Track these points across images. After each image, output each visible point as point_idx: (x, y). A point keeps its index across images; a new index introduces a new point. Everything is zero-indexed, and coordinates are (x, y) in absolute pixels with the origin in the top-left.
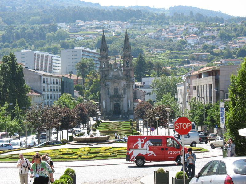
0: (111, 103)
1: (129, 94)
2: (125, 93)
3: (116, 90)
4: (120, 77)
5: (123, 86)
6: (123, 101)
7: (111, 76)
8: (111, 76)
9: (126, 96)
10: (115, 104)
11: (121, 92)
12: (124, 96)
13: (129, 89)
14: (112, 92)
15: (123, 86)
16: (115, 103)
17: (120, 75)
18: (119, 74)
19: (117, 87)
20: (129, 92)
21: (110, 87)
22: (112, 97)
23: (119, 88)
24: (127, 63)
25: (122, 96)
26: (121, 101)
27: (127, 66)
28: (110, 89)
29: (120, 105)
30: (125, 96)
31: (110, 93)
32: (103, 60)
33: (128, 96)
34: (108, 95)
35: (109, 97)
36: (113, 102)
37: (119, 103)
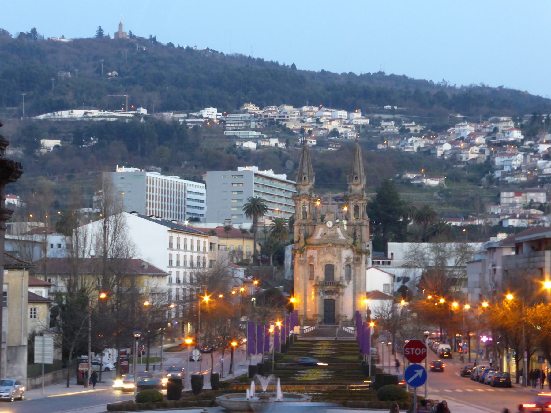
0: (318, 297)
2: (348, 277)
3: (329, 269)
4: (338, 241)
5: (344, 260)
6: (343, 294)
9: (351, 282)
10: (325, 300)
11: (340, 272)
12: (345, 283)
13: (358, 268)
14: (320, 273)
16: (327, 297)
18: (336, 233)
19: (331, 263)
20: (357, 277)
21: (316, 260)
22: (320, 286)
23: (335, 264)
25: (341, 283)
26: (339, 295)
28: (316, 266)
29: (336, 302)
30: (348, 283)
31: (316, 275)
32: (301, 202)
34: (310, 279)
35: (314, 284)
36: (322, 295)
37: (334, 297)
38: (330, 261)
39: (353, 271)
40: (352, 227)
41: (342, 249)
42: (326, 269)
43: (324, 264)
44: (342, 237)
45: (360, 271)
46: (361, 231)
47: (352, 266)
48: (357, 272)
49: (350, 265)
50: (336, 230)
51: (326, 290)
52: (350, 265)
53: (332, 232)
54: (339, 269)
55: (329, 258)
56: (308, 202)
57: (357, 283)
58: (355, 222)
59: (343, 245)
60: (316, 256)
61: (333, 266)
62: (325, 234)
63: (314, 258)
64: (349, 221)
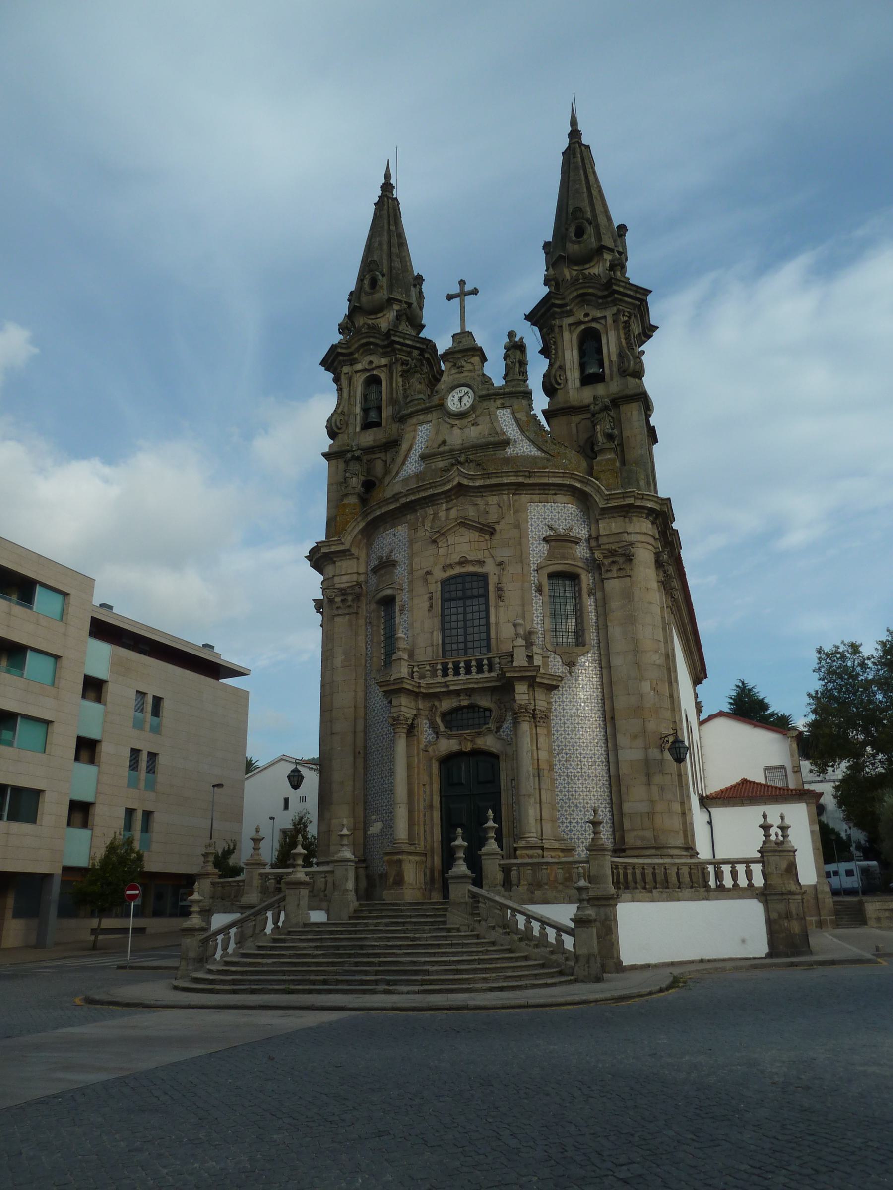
1: (619, 644)
5: (537, 552)
6: (540, 718)
7: (412, 466)
8: (412, 466)
11: (522, 614)
12: (556, 666)
15: (544, 548)
16: (448, 745)
17: (506, 443)
19: (471, 569)
20: (615, 631)
21: (401, 572)
23: (490, 568)
24: (590, 342)
27: (588, 380)
29: (504, 766)
32: (359, 367)
33: (605, 666)
37: (488, 742)
38: (463, 562)
39: (590, 604)
40: (576, 419)
42: (444, 600)
43: (439, 575)
44: (524, 448)
45: (628, 596)
46: (618, 423)
47: (586, 580)
48: (615, 604)
49: (573, 577)
50: (493, 420)
51: (446, 705)
52: (573, 577)
53: (474, 434)
54: (512, 590)
55: (463, 545)
56: (383, 361)
57: (617, 661)
58: (587, 395)
61: (484, 577)
62: (444, 442)
64: (560, 395)
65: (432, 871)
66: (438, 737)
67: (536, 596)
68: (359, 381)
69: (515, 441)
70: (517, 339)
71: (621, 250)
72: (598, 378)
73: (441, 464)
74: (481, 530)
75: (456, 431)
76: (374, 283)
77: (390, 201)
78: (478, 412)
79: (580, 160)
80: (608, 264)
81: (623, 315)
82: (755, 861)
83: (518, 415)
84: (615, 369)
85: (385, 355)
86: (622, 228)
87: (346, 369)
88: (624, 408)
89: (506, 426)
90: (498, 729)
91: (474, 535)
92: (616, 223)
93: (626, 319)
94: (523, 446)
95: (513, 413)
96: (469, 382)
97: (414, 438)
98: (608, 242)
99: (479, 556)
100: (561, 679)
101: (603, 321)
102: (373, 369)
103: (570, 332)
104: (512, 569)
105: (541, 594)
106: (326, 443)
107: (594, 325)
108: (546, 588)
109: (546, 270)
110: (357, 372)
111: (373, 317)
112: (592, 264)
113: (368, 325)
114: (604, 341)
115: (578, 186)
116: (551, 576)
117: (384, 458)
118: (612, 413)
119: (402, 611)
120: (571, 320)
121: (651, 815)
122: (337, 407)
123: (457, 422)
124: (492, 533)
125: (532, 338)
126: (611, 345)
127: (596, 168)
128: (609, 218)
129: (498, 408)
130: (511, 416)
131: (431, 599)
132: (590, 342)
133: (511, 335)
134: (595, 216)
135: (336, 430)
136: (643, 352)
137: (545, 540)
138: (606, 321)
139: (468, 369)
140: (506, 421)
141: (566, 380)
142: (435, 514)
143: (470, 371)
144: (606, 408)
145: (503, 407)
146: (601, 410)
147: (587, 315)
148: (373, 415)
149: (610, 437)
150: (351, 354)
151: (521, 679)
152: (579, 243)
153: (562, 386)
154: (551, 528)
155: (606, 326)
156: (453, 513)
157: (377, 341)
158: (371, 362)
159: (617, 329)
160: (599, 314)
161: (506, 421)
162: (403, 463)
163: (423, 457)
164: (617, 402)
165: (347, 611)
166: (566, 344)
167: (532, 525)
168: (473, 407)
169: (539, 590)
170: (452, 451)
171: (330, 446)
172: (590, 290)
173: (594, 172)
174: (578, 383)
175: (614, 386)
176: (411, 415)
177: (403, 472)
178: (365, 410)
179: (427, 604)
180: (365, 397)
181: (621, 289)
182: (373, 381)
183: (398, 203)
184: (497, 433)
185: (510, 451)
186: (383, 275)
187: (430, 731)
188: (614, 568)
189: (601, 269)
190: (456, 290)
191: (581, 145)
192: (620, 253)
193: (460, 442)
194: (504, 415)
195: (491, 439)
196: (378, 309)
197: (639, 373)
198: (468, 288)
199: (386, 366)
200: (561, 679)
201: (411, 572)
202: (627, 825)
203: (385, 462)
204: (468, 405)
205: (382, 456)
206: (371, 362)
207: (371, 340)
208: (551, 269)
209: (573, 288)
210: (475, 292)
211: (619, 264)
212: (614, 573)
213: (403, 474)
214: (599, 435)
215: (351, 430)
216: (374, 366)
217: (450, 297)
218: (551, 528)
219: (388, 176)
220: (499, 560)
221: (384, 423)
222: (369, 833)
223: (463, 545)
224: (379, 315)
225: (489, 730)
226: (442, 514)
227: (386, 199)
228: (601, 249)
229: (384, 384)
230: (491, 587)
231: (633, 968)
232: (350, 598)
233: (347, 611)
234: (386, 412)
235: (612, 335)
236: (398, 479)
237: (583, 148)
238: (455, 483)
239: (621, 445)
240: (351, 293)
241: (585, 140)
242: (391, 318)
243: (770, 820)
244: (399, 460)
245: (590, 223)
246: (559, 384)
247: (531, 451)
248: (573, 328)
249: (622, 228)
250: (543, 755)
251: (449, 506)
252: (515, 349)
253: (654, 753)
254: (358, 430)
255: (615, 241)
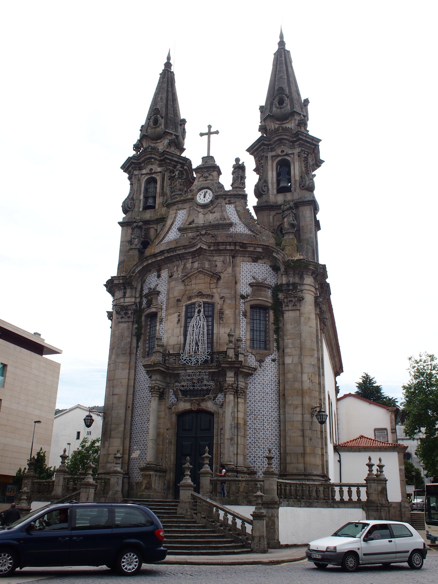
7: (173, 235)
8: (173, 235)
10: (181, 415)
12: (252, 361)
16: (184, 406)
17: (231, 225)
21: (162, 298)
24: (284, 167)
27: (281, 190)
30: (261, 361)
32: (144, 171)
33: (281, 364)
36: (172, 398)
37: (209, 406)
40: (273, 213)
41: (239, 259)
44: (240, 228)
45: (298, 322)
46: (296, 217)
50: (223, 210)
53: (212, 218)
56: (159, 169)
58: (280, 199)
59: (240, 249)
60: (163, 288)
62: (193, 221)
63: (158, 293)
64: (264, 198)
65: (169, 482)
66: (178, 401)
67: (242, 319)
68: (144, 179)
69: (236, 224)
70: (240, 163)
71: (305, 115)
72: (287, 190)
73: (190, 235)
74: (212, 276)
75: (201, 216)
76: (156, 122)
77: (169, 73)
78: (215, 205)
79: (283, 59)
80: (297, 122)
81: (304, 153)
82: (363, 486)
83: (238, 209)
84: (298, 185)
85: (160, 166)
86: (307, 101)
87: (136, 172)
88: (301, 209)
89: (230, 214)
90: (215, 398)
91: (208, 279)
92: (303, 98)
93: (305, 155)
94: (240, 228)
95: (235, 207)
96: (209, 186)
97: (175, 218)
98: (297, 109)
99: (209, 293)
100: (255, 369)
101: (292, 156)
102: (153, 174)
103: (273, 161)
104: (228, 301)
105: (245, 318)
106: (121, 216)
107: (286, 157)
108: (248, 314)
109: (261, 122)
110: (142, 174)
111: (155, 142)
112: (288, 121)
113: (151, 147)
114: (292, 168)
115: (282, 74)
116: (252, 307)
117: (156, 228)
118: (294, 211)
119: (161, 321)
120: (274, 153)
121: (304, 454)
122: (129, 195)
123: (202, 210)
124: (219, 279)
125: (250, 163)
126: (296, 170)
127: (293, 64)
128: (299, 95)
129: (226, 204)
130: (234, 209)
131: (179, 316)
132: (284, 167)
133: (237, 160)
134: (290, 92)
135: (128, 209)
136: (315, 175)
137: (251, 285)
138: (294, 156)
139: (210, 179)
140: (231, 212)
141: (268, 189)
142: (185, 265)
143: (211, 180)
144: (291, 208)
145: (230, 203)
146: (288, 209)
147: (282, 151)
148: (150, 201)
149: (293, 226)
150: (140, 163)
151: (230, 368)
152: (281, 108)
153: (266, 193)
154: (254, 278)
155: (294, 158)
156: (196, 265)
157: (157, 157)
158: (151, 169)
159: (300, 161)
160: (290, 152)
161: (231, 212)
162: (167, 232)
163: (180, 230)
164: (298, 204)
165: (127, 320)
166: (269, 168)
167: (242, 275)
168: (212, 202)
169: (245, 315)
170: (197, 227)
171: (124, 218)
172: (286, 137)
173: (292, 67)
174: (275, 191)
175: (296, 195)
176: (174, 204)
177: (167, 237)
178: (146, 198)
179: (177, 319)
180: (146, 190)
181: (304, 138)
182: (152, 181)
183: (174, 75)
184: (225, 219)
185: (232, 230)
186: (162, 118)
187: (173, 397)
188: (291, 305)
189: (293, 125)
190: (206, 131)
191: (285, 50)
192: (304, 116)
193: (202, 222)
194: (230, 208)
195: (221, 222)
196: (158, 138)
197: (311, 189)
198: (212, 130)
199: (160, 172)
200: (255, 369)
201: (168, 299)
202: (288, 460)
203: (157, 230)
204: (209, 200)
205: (155, 226)
206: (151, 169)
207: (153, 156)
208: (263, 122)
209: (276, 135)
210: (217, 132)
211: (303, 123)
212: (290, 308)
213: (167, 239)
214: (286, 223)
215: (136, 209)
216: (153, 171)
217: (202, 135)
218: (254, 278)
219: (169, 58)
220: (222, 295)
221: (157, 207)
222: (132, 456)
223: (200, 284)
224: (158, 141)
225: (210, 398)
226: (189, 265)
227: (167, 72)
228: (293, 113)
229: (159, 183)
230: (216, 311)
231: (287, 546)
232: (130, 312)
233: (127, 320)
234: (159, 200)
235: (297, 165)
236: (163, 242)
237: (286, 52)
238: (198, 247)
239: (298, 230)
240: (142, 127)
241: (287, 48)
242: (165, 144)
243: (373, 462)
244: (166, 229)
245: (288, 97)
246: (264, 191)
247: (245, 231)
248: (274, 158)
249: (307, 101)
250: (241, 415)
251: (194, 261)
252: (239, 169)
253: (307, 416)
254: (141, 210)
255: (302, 108)
